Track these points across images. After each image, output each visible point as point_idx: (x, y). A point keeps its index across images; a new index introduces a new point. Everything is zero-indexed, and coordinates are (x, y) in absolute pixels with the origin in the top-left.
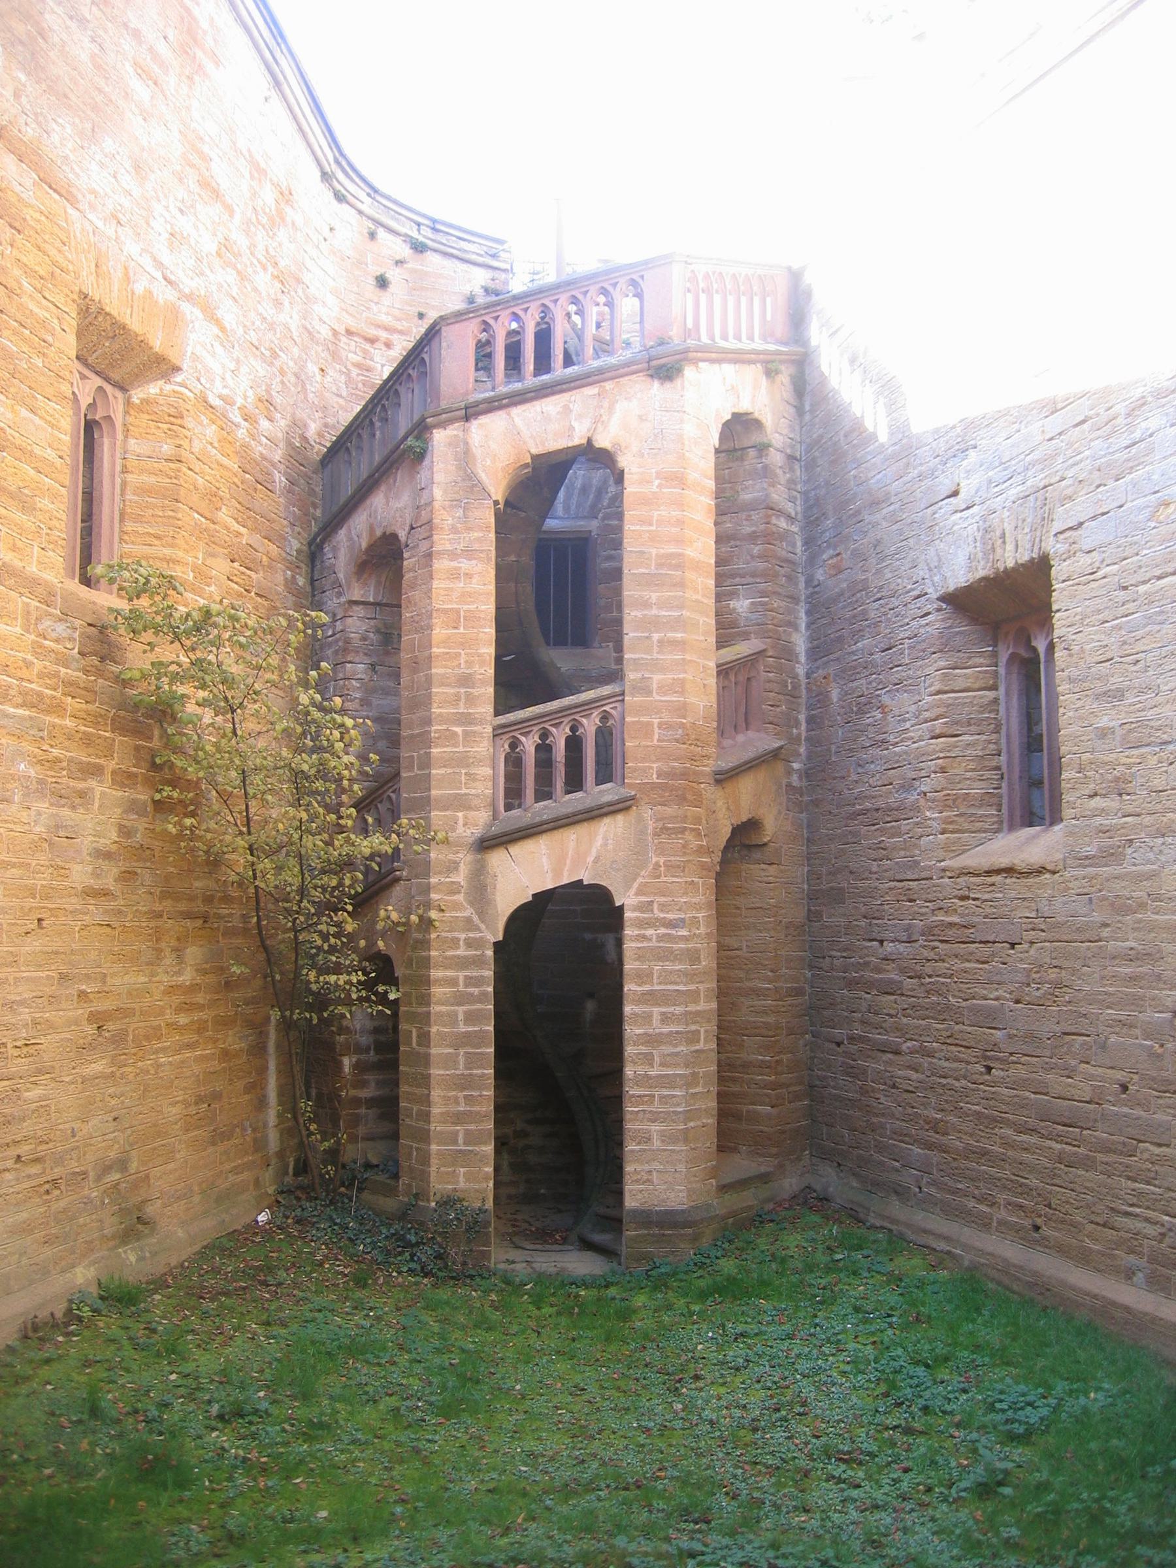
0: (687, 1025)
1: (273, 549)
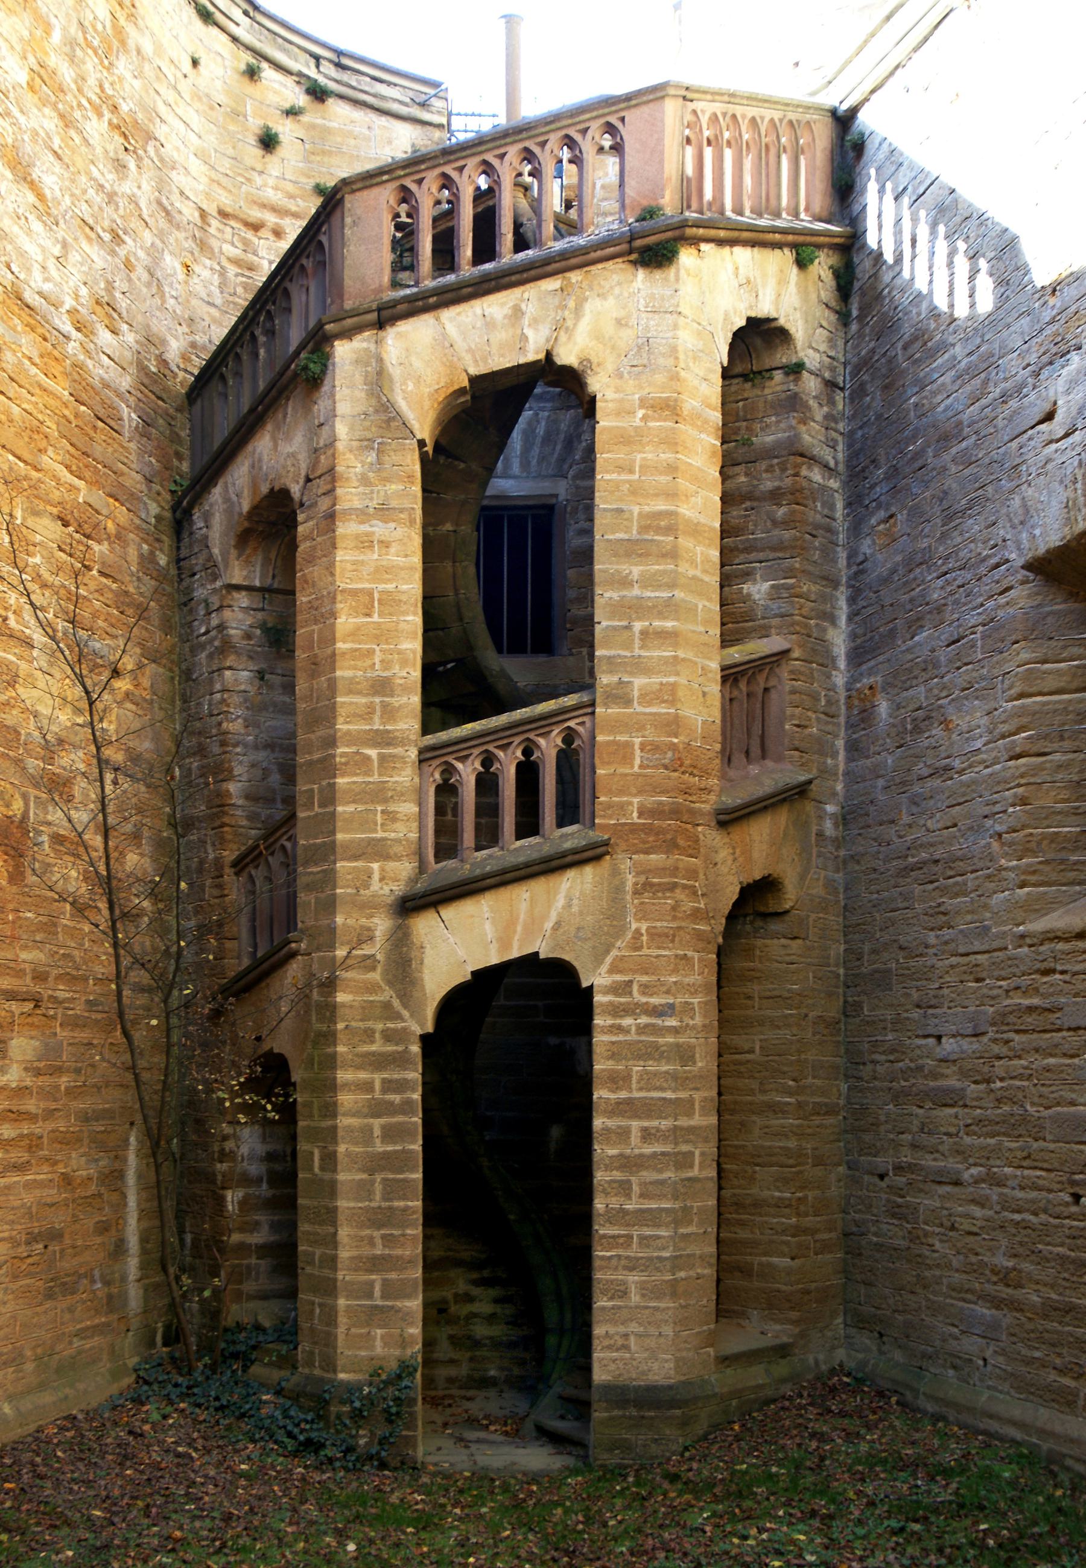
0: (676, 1144)
1: (122, 514)
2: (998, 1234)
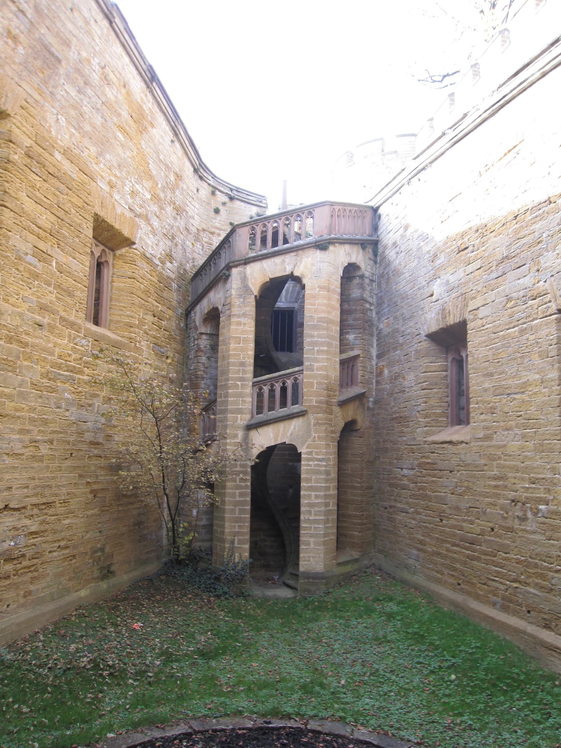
1: (170, 312)
2: (419, 529)
